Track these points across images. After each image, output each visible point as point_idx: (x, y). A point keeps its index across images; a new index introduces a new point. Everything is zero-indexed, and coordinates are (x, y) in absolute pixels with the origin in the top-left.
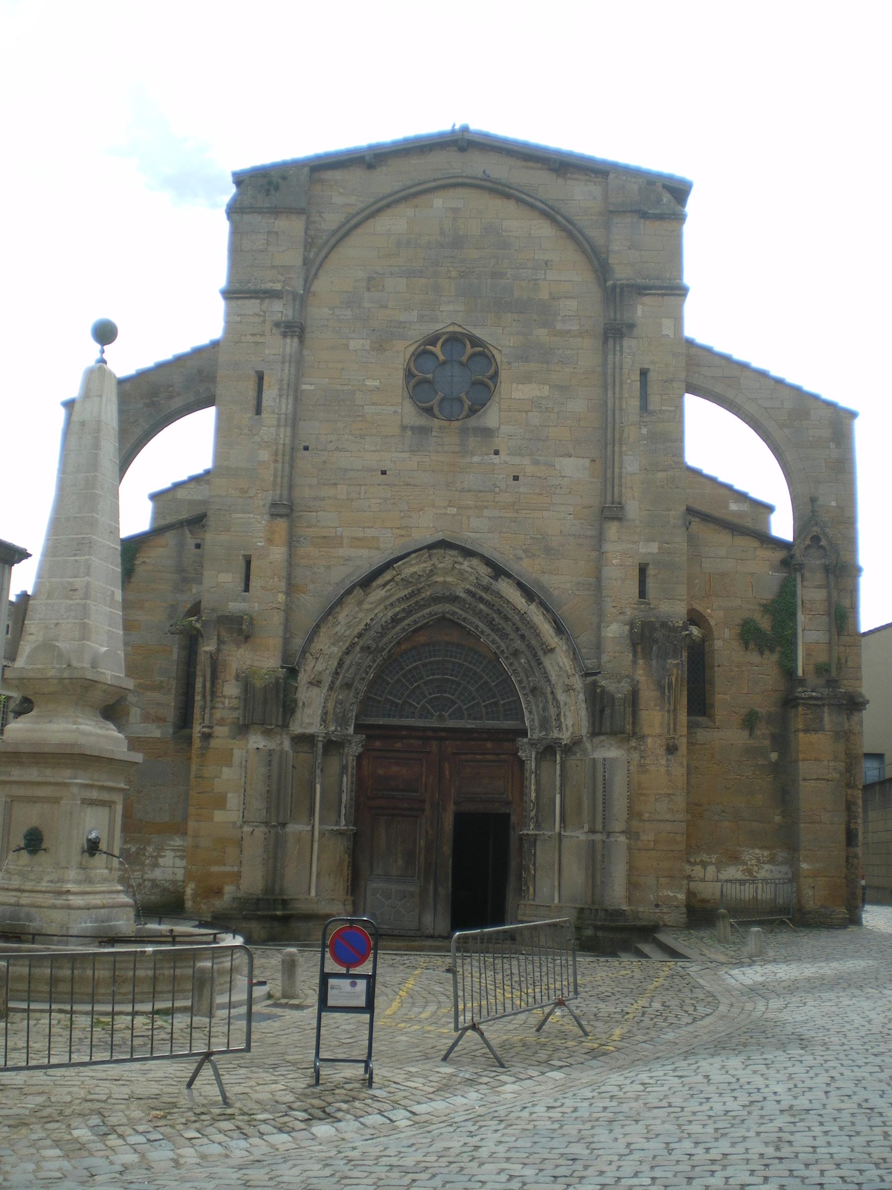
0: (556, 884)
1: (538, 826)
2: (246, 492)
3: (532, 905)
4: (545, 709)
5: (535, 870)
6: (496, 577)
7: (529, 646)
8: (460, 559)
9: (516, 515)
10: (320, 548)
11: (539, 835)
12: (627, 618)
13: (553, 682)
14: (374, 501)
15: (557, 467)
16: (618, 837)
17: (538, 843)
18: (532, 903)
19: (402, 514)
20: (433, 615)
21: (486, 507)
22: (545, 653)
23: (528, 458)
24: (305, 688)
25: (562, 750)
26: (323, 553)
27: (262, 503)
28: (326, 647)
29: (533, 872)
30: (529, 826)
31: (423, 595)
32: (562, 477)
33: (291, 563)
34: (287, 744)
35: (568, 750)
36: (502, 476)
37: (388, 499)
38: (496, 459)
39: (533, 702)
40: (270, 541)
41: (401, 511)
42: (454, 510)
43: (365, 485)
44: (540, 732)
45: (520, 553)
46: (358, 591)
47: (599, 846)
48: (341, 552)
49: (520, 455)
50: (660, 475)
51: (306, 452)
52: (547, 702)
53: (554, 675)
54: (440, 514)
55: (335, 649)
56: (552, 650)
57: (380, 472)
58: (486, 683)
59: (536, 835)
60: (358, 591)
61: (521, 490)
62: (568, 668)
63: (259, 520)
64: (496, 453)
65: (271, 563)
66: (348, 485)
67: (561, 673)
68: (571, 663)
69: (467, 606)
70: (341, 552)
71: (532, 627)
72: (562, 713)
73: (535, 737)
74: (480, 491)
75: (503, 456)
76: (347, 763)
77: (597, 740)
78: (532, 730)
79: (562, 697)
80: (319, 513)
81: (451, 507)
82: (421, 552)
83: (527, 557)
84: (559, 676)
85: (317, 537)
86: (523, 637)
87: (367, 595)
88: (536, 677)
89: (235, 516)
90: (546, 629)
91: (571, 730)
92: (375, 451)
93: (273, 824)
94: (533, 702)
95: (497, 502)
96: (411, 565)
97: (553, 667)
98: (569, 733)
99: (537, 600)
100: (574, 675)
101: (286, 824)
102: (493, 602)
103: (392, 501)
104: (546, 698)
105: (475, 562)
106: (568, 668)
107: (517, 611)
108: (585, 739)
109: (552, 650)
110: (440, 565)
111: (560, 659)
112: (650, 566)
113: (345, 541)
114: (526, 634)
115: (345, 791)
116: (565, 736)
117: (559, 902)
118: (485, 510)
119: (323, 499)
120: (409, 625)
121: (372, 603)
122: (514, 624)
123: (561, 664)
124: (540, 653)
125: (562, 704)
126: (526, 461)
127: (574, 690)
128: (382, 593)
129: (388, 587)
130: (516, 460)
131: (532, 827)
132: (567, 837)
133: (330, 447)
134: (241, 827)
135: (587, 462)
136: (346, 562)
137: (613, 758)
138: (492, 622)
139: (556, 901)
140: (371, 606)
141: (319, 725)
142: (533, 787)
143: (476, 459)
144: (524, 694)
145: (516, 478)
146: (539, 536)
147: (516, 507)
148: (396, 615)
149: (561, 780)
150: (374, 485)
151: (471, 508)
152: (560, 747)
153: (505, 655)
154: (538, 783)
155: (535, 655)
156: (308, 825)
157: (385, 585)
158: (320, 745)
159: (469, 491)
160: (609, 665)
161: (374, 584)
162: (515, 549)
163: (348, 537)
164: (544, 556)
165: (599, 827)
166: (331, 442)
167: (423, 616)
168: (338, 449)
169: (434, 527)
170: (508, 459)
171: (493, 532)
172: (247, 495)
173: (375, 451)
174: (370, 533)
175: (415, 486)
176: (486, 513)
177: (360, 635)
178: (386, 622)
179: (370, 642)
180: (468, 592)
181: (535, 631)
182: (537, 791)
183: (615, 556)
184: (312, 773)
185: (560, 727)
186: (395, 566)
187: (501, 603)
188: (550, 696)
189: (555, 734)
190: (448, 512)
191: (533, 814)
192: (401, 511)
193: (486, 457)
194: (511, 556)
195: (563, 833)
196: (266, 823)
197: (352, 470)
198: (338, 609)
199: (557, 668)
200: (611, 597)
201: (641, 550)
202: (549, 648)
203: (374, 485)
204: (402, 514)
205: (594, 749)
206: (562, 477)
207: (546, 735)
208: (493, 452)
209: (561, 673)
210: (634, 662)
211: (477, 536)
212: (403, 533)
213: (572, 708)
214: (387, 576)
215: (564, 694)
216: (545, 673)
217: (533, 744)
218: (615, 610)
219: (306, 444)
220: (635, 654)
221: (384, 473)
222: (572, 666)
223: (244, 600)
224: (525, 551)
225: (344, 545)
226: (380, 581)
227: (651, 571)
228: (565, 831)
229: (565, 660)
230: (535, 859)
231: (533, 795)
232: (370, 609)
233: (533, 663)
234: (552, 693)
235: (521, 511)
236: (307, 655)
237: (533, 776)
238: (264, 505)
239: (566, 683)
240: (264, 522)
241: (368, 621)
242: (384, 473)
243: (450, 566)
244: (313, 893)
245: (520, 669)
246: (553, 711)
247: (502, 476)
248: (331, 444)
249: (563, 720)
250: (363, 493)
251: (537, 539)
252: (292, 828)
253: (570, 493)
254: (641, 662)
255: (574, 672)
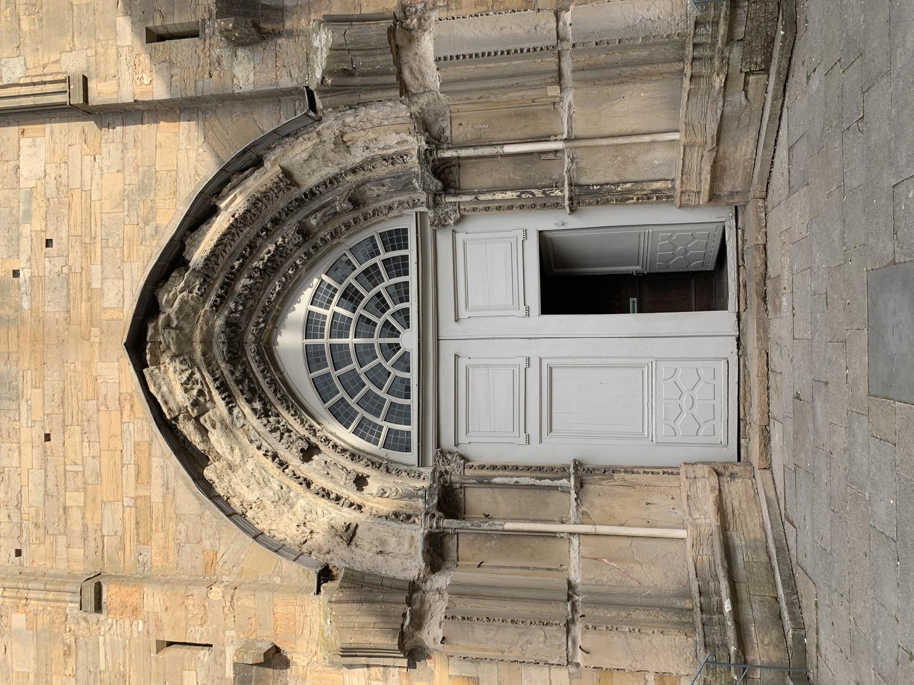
0: (647, 139)
1: (558, 185)
2: (69, 647)
3: (682, 183)
4: (380, 182)
5: (625, 183)
6: (185, 264)
7: (289, 211)
8: (162, 317)
9: (98, 240)
10: (152, 530)
11: (570, 178)
12: (226, 53)
13: (337, 171)
14: (86, 451)
15: (32, 184)
16: (565, 24)
17: (584, 180)
18: (678, 182)
19: (102, 408)
20: (262, 358)
21: (89, 284)
22: (295, 184)
23: (21, 226)
24: (358, 550)
25: (438, 149)
26: (160, 526)
27: (83, 623)
28: (294, 518)
29: (628, 185)
30: (557, 197)
31: (226, 372)
32: (45, 176)
33: (164, 582)
34: (441, 581)
35: (435, 140)
36: (47, 264)
37: (82, 430)
38: (24, 274)
39: (375, 205)
40: (135, 611)
41: (99, 410)
42: (95, 330)
43: (65, 464)
44: (415, 189)
45: (149, 230)
46: (208, 473)
47: (583, 59)
48: (157, 498)
49: (18, 240)
50: (25, 26)
51: (24, 553)
52: (368, 181)
53: (327, 169)
54: (100, 351)
55: (301, 502)
56: (287, 174)
57: (48, 443)
58: (356, 278)
59: (570, 185)
60: (208, 473)
61: (64, 234)
62: (310, 144)
63: (108, 627)
64: (16, 274)
65: (166, 609)
66: (66, 491)
67: (319, 155)
68: (301, 139)
69: (240, 308)
70: (156, 498)
71: (255, 204)
72: (384, 152)
73: (423, 197)
74: (68, 295)
75: (20, 264)
76: (475, 477)
77: (413, 86)
78: (415, 205)
79: (358, 156)
80: (105, 533)
81: (90, 336)
82: (148, 378)
83: (154, 218)
84: (326, 160)
85: (138, 534)
86: (276, 221)
87: (218, 457)
88: (334, 201)
89: (102, 667)
90: (257, 182)
91: (404, 136)
92: (20, 451)
93: (569, 608)
94: (375, 205)
95: (82, 268)
96: (171, 392)
97: (314, 171)
98: (410, 138)
99: (214, 199)
100: (319, 134)
101: (569, 583)
102: (228, 269)
103: (86, 424)
104: (364, 183)
105: (164, 298)
106: (310, 144)
107: (234, 230)
108: (414, 109)
109: (287, 174)
110: (173, 347)
111: (298, 158)
112: (150, 25)
113: (141, 493)
114: (270, 216)
115: (516, 479)
116: (415, 144)
117: (678, 131)
118: (93, 286)
119: (85, 526)
120: (275, 391)
121: (232, 449)
122: (258, 235)
123: (305, 155)
124: (296, 193)
125: (367, 154)
126: (26, 229)
127: (343, 134)
128: (216, 437)
129: (208, 426)
130: (25, 245)
131: (559, 193)
132: (570, 127)
133: (15, 519)
134: (578, 665)
135: (25, 142)
136: (171, 491)
137: (435, 44)
138: (260, 270)
139: (676, 136)
140: (237, 451)
141: (413, 526)
142: (499, 196)
143: (26, 305)
144: (365, 219)
145: (49, 243)
146: (126, 203)
147: (88, 241)
148: (254, 410)
149: (482, 146)
150: (64, 452)
151: (91, 307)
152: (431, 152)
153: (311, 250)
154: (492, 191)
155: (300, 202)
156: (570, 541)
157: (203, 431)
158: (446, 523)
159: (68, 311)
160: (295, 75)
161: (200, 447)
162: (144, 239)
163: (136, 488)
164: (152, 194)
165: (550, 62)
166: (9, 516)
167: (262, 372)
168: (18, 507)
169: (118, 361)
170: (24, 257)
171: (122, 271)
172: (74, 646)
173: (20, 451)
174: (129, 457)
175: (63, 391)
176: (96, 284)
177: (283, 465)
178: (265, 425)
179: (294, 450)
180: (216, 307)
181: (258, 199)
182: (504, 190)
183: (138, 81)
184: (488, 535)
185: (402, 155)
186: (168, 417)
187: (226, 256)
188: (360, 176)
189: (413, 161)
190: (97, 340)
191: (538, 193)
192: (99, 410)
193: (23, 289)
194: (154, 243)
195: (565, 136)
196: (569, 625)
197: (46, 486)
198: (235, 503)
199: (314, 164)
200: (196, 81)
201: (129, 43)
202: (281, 176)
203: (64, 452)
204: (102, 408)
205: (427, 90)
206: (45, 176)
207: (417, 177)
208: (15, 279)
209: (319, 155)
210: (290, 34)
211: (127, 294)
212: (127, 407)
213: (371, 135)
214: (188, 429)
215: (353, 150)
216: (324, 183)
217: (434, 201)
218: (215, 73)
219: (13, 553)
220: (279, 34)
221: (47, 437)
222: (306, 136)
223: (223, 652)
224: (146, 224)
225: (147, 493)
226: (195, 438)
227: (157, 23)
228: (562, 134)
229: (298, 149)
230: (607, 184)
231: (509, 195)
232: (240, 449)
233: (315, 205)
234: (354, 171)
235: (93, 233)
236: (304, 550)
237: (482, 197)
238: (85, 620)
239: (332, 146)
240: (110, 621)
241: (261, 452)
242: (47, 437)
243: (173, 333)
244: (682, 533)
245: (330, 228)
246: (382, 170)
247: (47, 264)
248: (12, 515)
249: (391, 151)
250: (80, 468)
251: (129, 206)
252: (576, 577)
253: (65, 163)
254: (288, 24)
255: (315, 135)
